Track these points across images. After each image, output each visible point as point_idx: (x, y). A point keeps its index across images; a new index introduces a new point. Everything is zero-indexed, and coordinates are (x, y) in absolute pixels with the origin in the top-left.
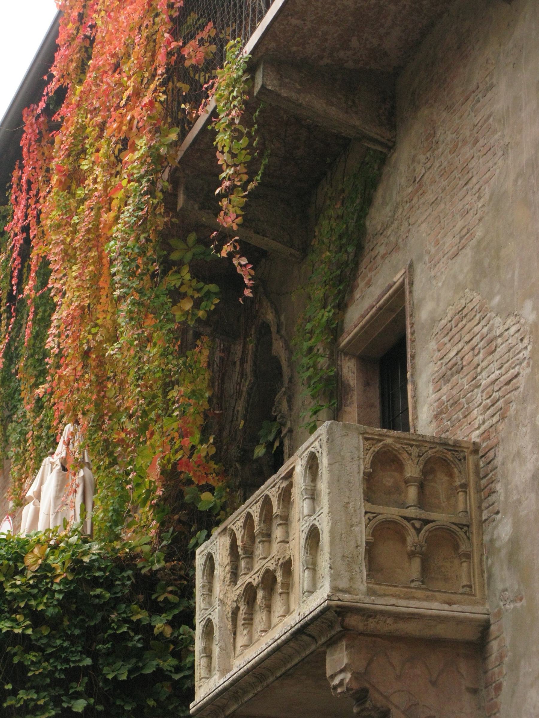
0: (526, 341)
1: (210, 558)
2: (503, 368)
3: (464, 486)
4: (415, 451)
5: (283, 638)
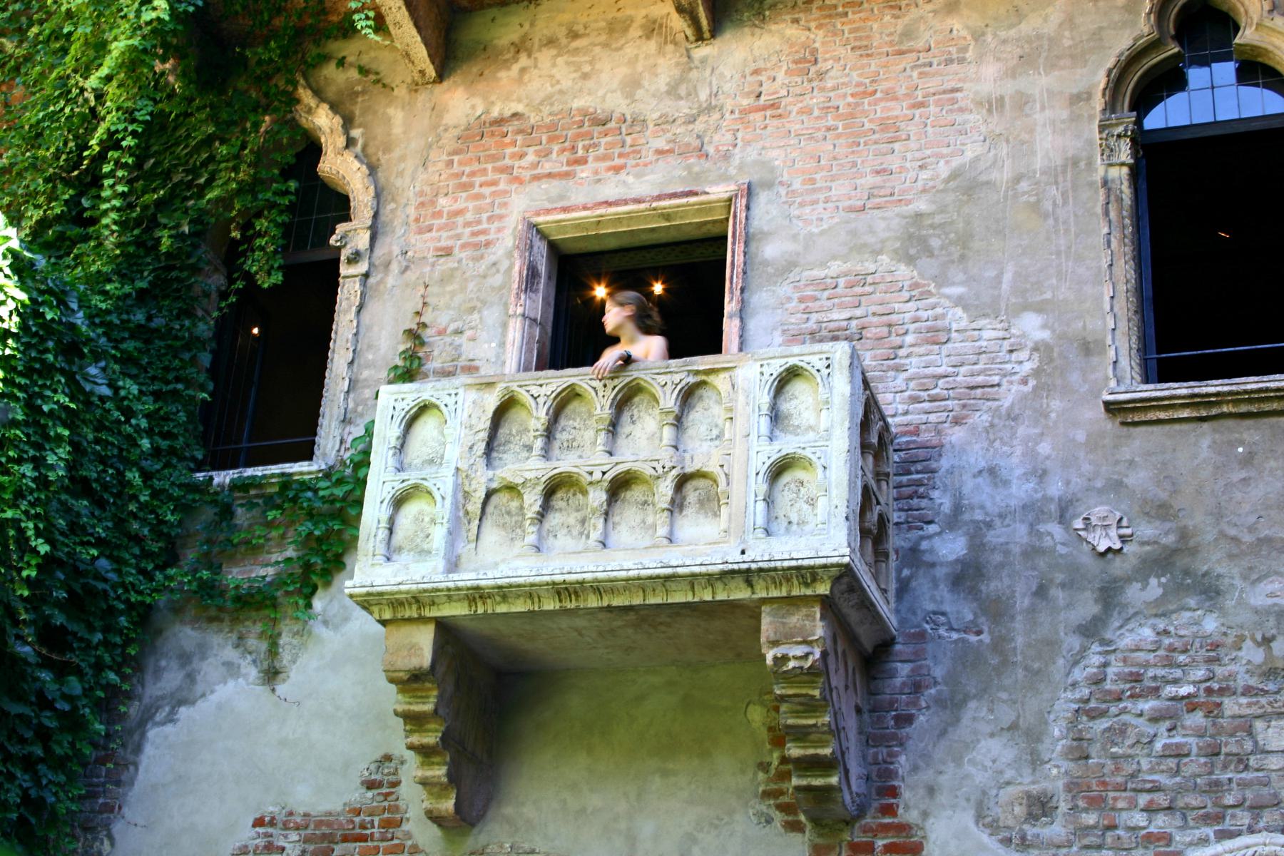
0: (1023, 355)
2: (963, 370)
5: (697, 570)
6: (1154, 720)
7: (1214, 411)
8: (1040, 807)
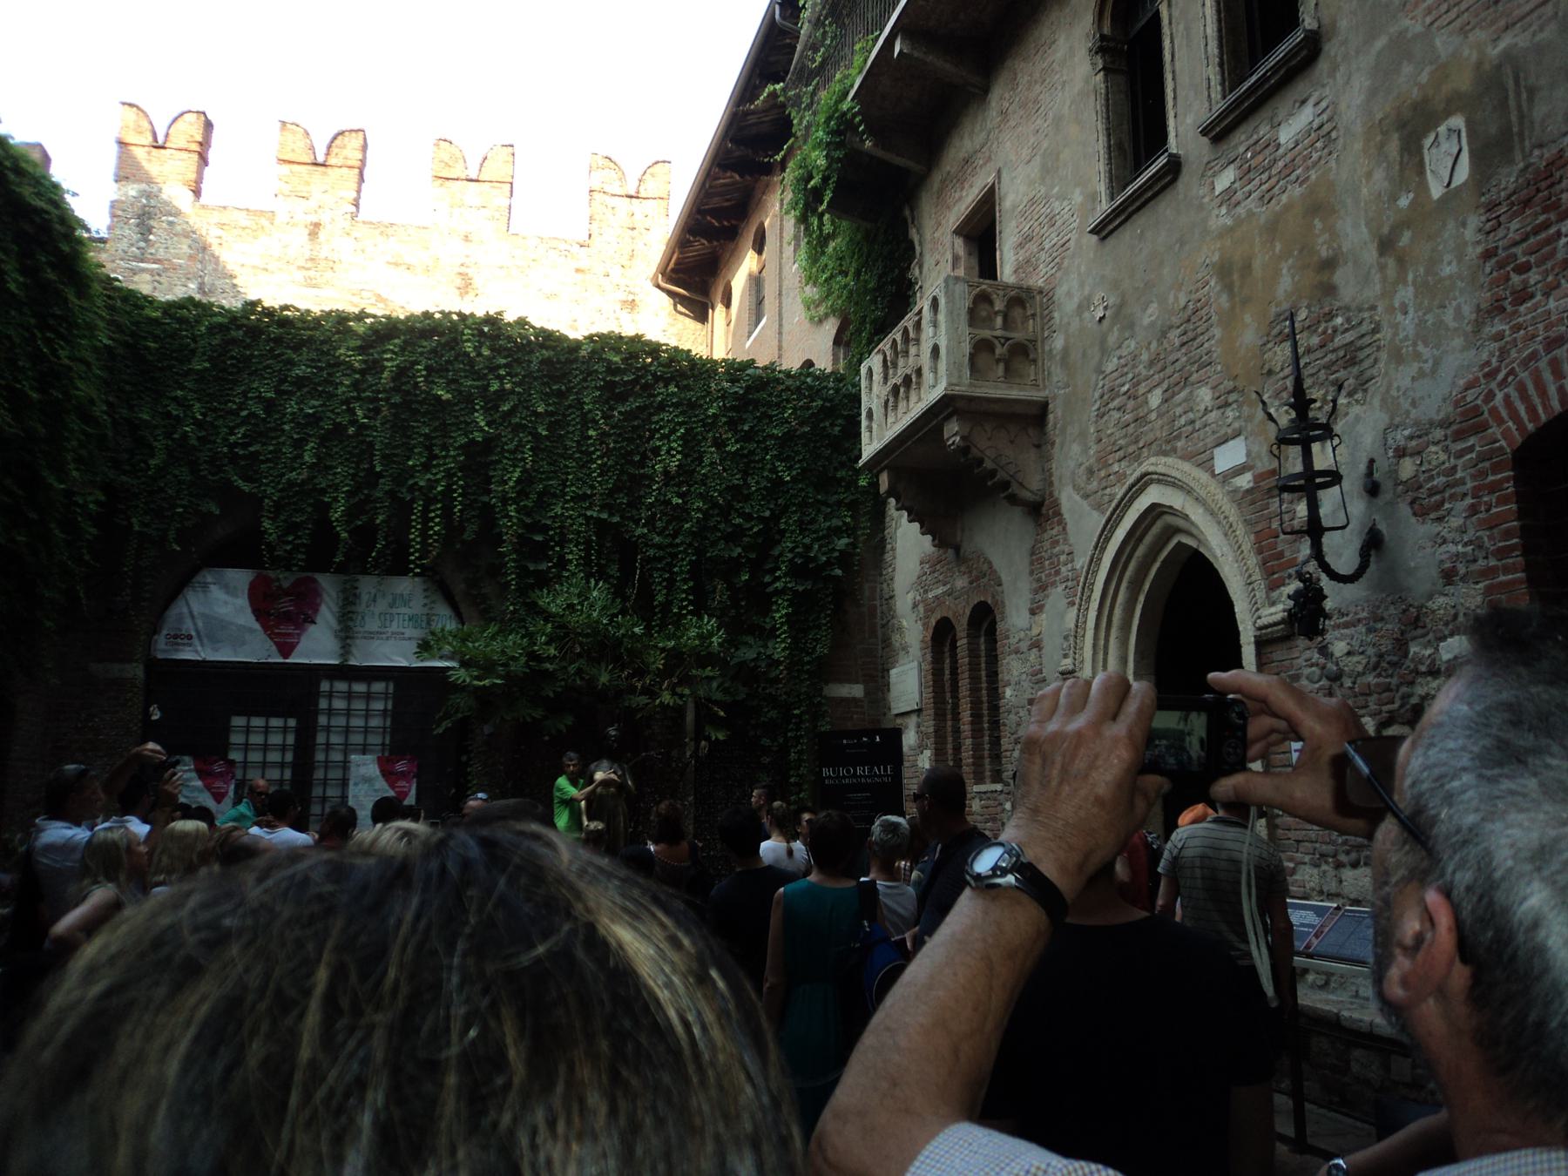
1: (870, 369)
3: (1033, 315)
4: (1002, 293)
6: (1119, 409)
7: (1126, 214)
8: (1090, 472)
